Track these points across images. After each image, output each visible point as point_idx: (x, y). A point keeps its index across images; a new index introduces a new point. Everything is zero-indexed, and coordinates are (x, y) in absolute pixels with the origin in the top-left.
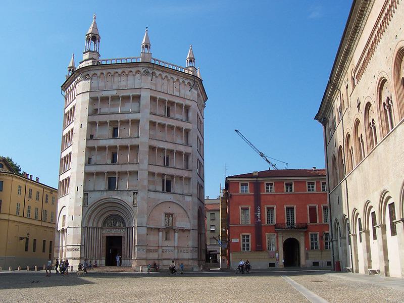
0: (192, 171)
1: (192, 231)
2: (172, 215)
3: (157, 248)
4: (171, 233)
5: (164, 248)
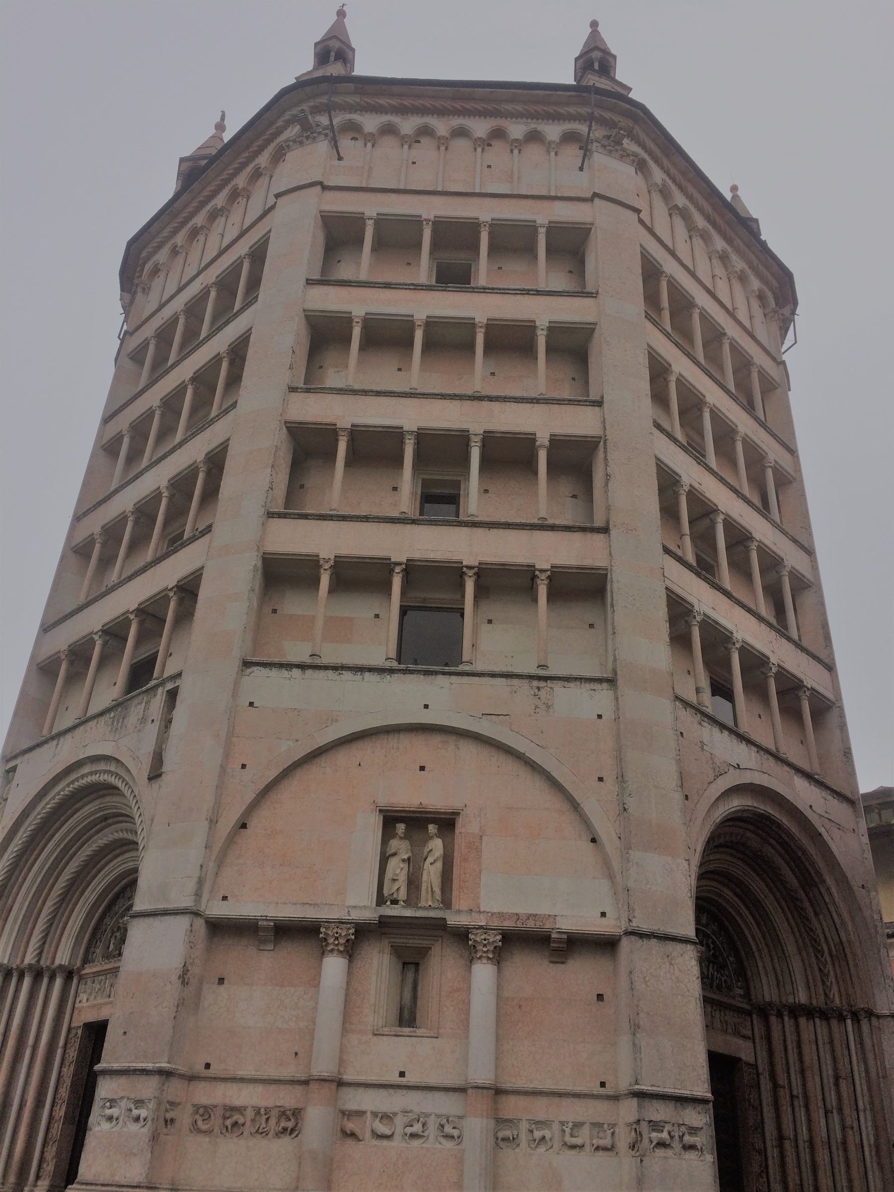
0: (605, 530)
1: (626, 944)
2: (447, 823)
3: (287, 1098)
4: (443, 965)
5: (355, 1100)
